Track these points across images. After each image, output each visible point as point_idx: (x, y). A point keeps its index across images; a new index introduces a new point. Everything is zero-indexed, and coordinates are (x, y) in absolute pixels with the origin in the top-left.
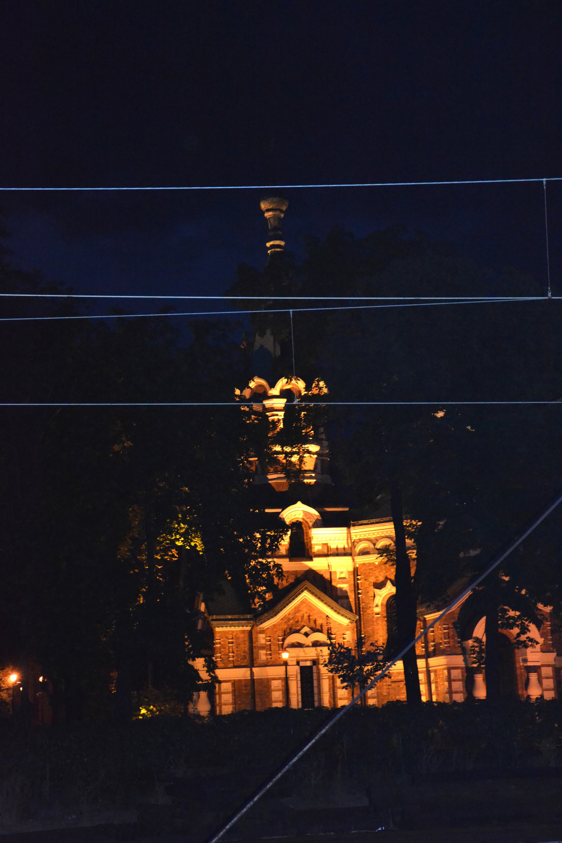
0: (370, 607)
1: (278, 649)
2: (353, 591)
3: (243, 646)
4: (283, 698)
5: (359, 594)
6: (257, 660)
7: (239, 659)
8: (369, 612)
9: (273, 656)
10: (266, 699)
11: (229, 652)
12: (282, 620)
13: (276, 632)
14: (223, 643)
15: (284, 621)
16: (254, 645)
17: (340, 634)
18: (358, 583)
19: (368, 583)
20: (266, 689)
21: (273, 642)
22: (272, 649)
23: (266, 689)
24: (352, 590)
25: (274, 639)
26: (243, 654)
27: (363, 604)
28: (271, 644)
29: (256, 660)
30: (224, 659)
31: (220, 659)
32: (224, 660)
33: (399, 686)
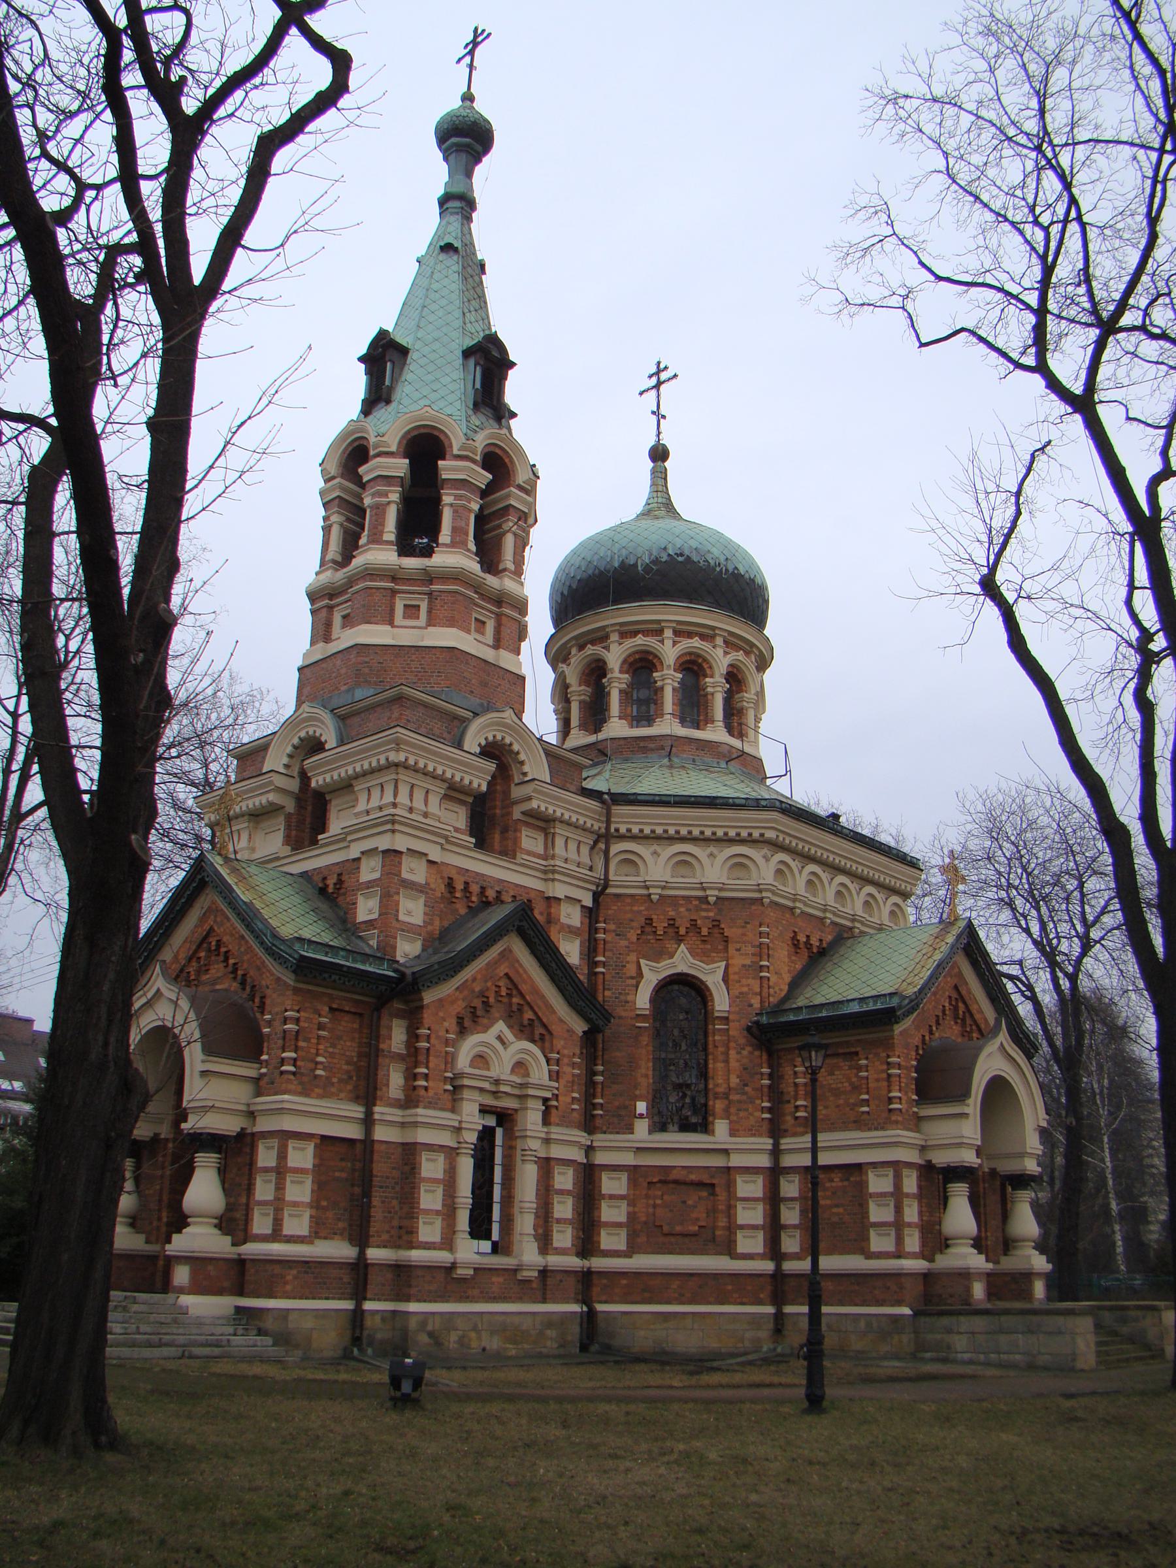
0: (627, 1002)
3: (348, 1044)
5: (596, 964)
7: (335, 1080)
8: (623, 1014)
9: (431, 1084)
11: (317, 1055)
14: (306, 1025)
15: (461, 996)
16: (382, 1046)
17: (569, 1057)
18: (596, 940)
19: (625, 943)
22: (431, 1065)
25: (438, 1037)
26: (345, 1067)
27: (607, 993)
28: (431, 1052)
30: (302, 1070)
31: (292, 1068)
32: (302, 1074)
33: (684, 1202)
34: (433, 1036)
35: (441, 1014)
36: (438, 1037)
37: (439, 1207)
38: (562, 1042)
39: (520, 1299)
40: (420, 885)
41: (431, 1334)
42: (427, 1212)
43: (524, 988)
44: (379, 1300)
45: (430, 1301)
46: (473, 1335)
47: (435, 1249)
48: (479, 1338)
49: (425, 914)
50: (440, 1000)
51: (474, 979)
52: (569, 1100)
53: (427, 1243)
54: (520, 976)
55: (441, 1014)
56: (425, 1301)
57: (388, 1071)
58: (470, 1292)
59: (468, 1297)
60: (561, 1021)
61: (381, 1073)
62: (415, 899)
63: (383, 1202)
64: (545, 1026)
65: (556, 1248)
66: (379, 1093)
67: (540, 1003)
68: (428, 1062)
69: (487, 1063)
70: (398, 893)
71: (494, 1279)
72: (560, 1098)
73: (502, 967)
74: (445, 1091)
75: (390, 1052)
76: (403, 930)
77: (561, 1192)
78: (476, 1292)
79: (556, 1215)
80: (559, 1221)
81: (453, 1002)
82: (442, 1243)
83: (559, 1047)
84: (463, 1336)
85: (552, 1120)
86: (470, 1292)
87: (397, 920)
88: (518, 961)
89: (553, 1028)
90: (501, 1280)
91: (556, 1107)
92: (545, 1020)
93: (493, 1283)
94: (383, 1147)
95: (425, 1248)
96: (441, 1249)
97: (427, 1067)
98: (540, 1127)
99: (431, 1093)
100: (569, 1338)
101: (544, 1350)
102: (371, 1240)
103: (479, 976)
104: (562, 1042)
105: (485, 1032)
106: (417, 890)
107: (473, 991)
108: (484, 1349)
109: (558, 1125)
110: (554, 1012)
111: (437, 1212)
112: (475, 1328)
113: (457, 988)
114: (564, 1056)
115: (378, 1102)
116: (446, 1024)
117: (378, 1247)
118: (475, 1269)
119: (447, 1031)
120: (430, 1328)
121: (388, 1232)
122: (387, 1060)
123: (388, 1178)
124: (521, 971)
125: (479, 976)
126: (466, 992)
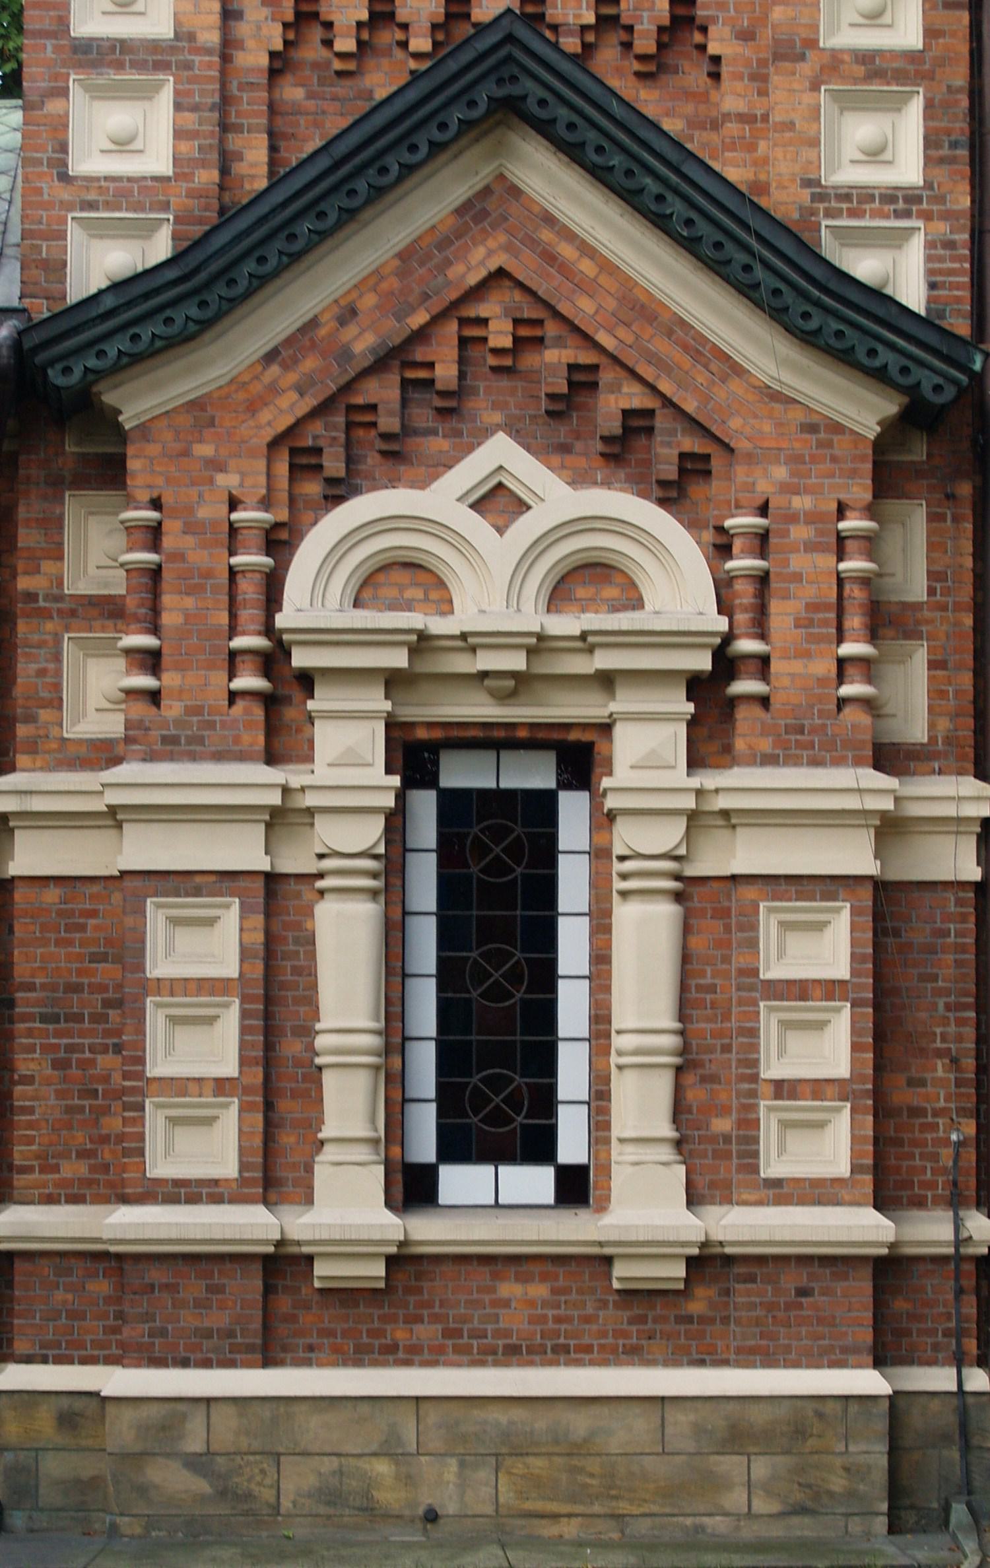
1: (223, 618)
2: (963, 153)
4: (243, 1061)
6: (44, 715)
9: (170, 679)
10: (106, 1061)
12: (275, 369)
13: (217, 465)
15: (292, 377)
16: (24, 583)
17: (812, 518)
20: (106, 972)
21: (179, 556)
23: (106, 972)
24: (954, 145)
29: (31, 719)
34: (172, 527)
35: (205, 450)
36: (191, 528)
37: (229, 1068)
38: (781, 473)
39: (634, 1355)
40: (154, 46)
41: (197, 1464)
42: (179, 1086)
43: (583, 308)
44: (60, 1360)
45: (206, 1364)
46: (382, 1468)
47: (217, 1199)
48: (408, 1480)
49: (179, 134)
50: (196, 405)
51: (348, 314)
52: (825, 667)
53: (178, 1183)
54: (565, 270)
55: (205, 450)
56: (185, 1363)
57: (57, 658)
58: (400, 1334)
59: (392, 1349)
60: (776, 396)
61: (26, 670)
62: (147, 93)
63: (57, 1065)
64: (696, 426)
65: (777, 1183)
66: (22, 731)
67: (661, 346)
68: (155, 610)
69: (441, 584)
70: (64, 93)
71: (509, 1289)
72: (775, 666)
73: (479, 253)
74: (233, 696)
75: (60, 598)
76: (91, 206)
77: (800, 990)
78: (426, 1332)
79: (773, 1069)
80: (784, 1089)
81: (252, 407)
82: (242, 1181)
83: (764, 487)
84: (340, 1472)
85: (740, 745)
86: (400, 1334)
87: (64, 177)
88: (549, 220)
89: (735, 427)
90: (539, 1290)
91: (764, 701)
92: (690, 406)
93: (506, 1303)
94: (52, 895)
95: (172, 1199)
96: (234, 1200)
97: (155, 630)
98: (679, 776)
99: (172, 709)
100: (838, 1483)
101: (717, 1524)
102: (19, 1180)
103: (369, 301)
104: (781, 473)
105: (422, 484)
106: (139, 66)
107: (345, 354)
108: (432, 1517)
109: (769, 760)
110: (738, 370)
111: (221, 1086)
112: (390, 1449)
113: (271, 357)
114: (793, 518)
115: (22, 759)
116: (228, 481)
117: (50, 1200)
118: (391, 1260)
119: (234, 504)
120: (194, 1444)
121: (83, 1154)
122: (49, 626)
123: (76, 988)
124: (567, 251)
125: (369, 301)
126: (310, 364)
